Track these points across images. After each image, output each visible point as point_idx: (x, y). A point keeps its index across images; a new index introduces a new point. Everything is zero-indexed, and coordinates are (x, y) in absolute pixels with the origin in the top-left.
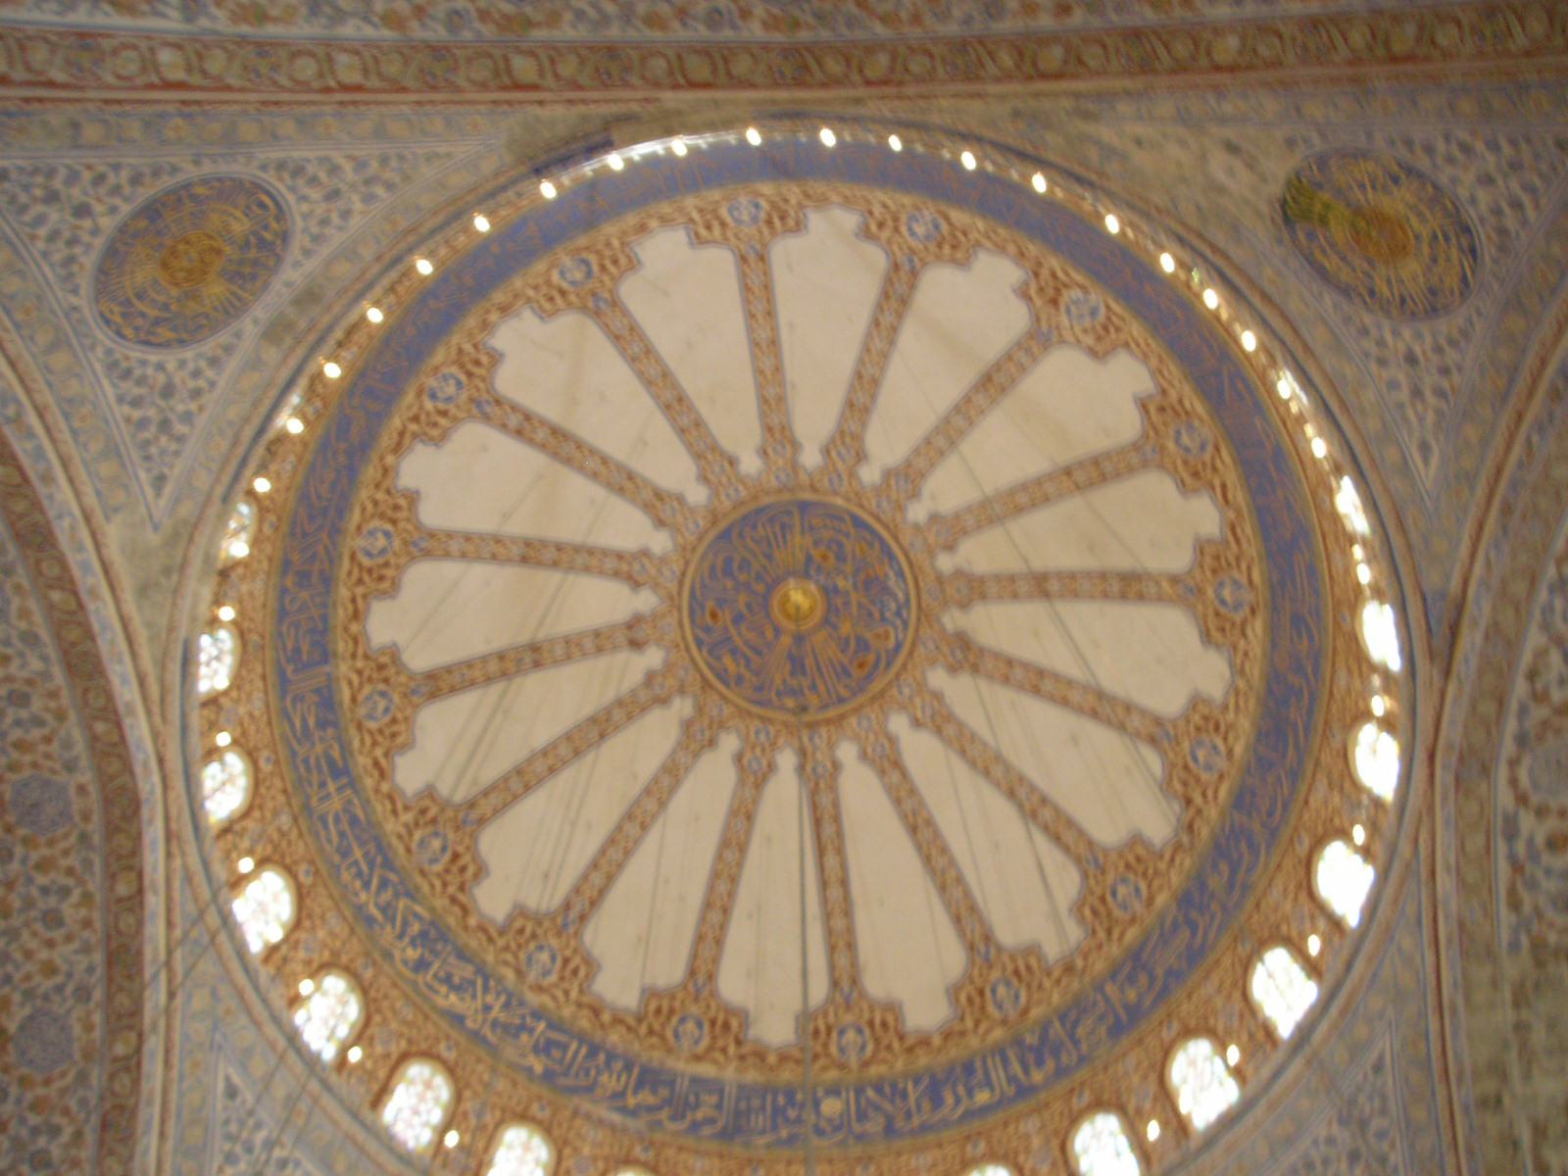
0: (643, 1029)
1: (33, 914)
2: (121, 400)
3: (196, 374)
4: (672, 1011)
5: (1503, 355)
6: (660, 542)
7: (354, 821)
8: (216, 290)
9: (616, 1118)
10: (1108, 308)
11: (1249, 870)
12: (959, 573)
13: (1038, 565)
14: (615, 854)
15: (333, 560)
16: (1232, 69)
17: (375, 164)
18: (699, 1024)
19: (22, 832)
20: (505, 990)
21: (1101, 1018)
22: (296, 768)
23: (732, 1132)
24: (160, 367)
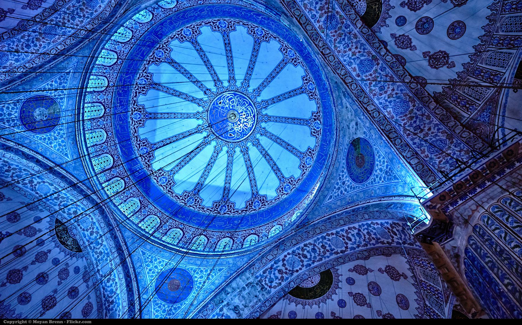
0: (138, 143)
4: (146, 145)
7: (136, 64)
9: (119, 149)
11: (242, 226)
12: (258, 140)
15: (178, 27)
16: (368, 111)
21: (198, 220)
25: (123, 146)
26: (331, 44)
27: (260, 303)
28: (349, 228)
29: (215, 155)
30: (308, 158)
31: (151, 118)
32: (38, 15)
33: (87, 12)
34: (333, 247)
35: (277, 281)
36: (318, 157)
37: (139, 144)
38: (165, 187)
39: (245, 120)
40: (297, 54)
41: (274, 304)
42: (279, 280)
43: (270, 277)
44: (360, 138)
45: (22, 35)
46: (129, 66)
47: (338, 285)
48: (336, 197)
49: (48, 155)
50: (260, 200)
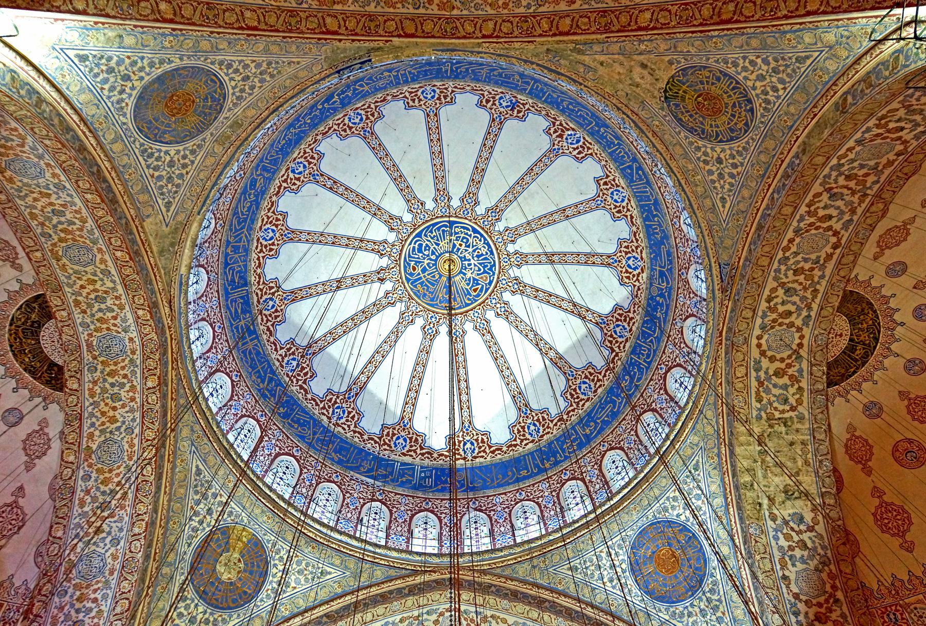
1: (106, 395)
2: (148, 167)
3: (184, 157)
4: (394, 434)
5: (763, 158)
6: (392, 237)
7: (258, 353)
8: (193, 119)
9: (369, 480)
10: (584, 138)
12: (516, 253)
13: (549, 250)
14: (371, 367)
17: (264, 65)
18: (405, 440)
19: (101, 359)
20: (323, 426)
22: (233, 331)
23: (420, 487)
24: (167, 153)
25: (369, 471)
26: (482, 10)
27: (809, 447)
28: (809, 206)
29: (488, 337)
30: (612, 193)
31: (357, 394)
32: (63, 452)
33: (123, 368)
34: (813, 257)
35: (792, 390)
36: (625, 177)
37: (385, 444)
38: (482, 454)
39: (471, 250)
40: (438, 84)
41: (829, 425)
42: (792, 386)
43: (775, 396)
44: (673, 77)
45: (77, 502)
46: (253, 369)
47: (884, 296)
48: (730, 191)
49: (302, 604)
50: (617, 320)
